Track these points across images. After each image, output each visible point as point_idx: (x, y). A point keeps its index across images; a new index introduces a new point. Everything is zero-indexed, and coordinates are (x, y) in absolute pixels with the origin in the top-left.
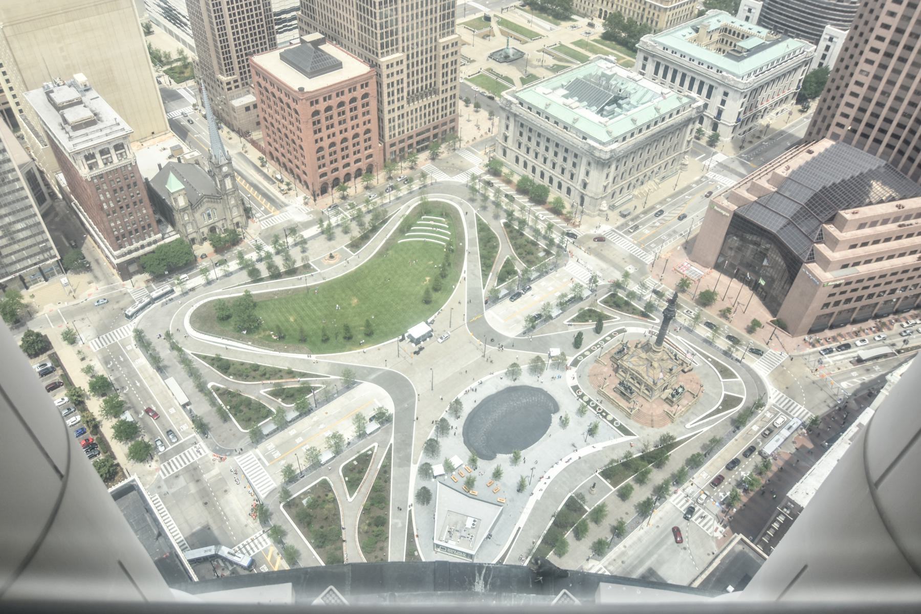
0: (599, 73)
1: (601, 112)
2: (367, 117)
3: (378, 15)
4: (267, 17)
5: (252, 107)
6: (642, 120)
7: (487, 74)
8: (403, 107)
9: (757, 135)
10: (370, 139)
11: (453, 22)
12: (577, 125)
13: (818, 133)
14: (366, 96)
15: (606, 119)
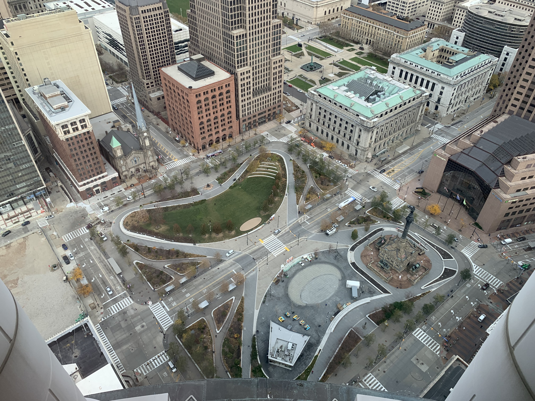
0: (366, 77)
1: (367, 100)
2: (229, 105)
3: (235, 44)
4: (170, 45)
5: (161, 98)
6: (392, 105)
8: (250, 98)
9: (463, 112)
10: (231, 117)
11: (280, 48)
12: (352, 108)
13: (500, 110)
14: (228, 92)
15: (371, 104)
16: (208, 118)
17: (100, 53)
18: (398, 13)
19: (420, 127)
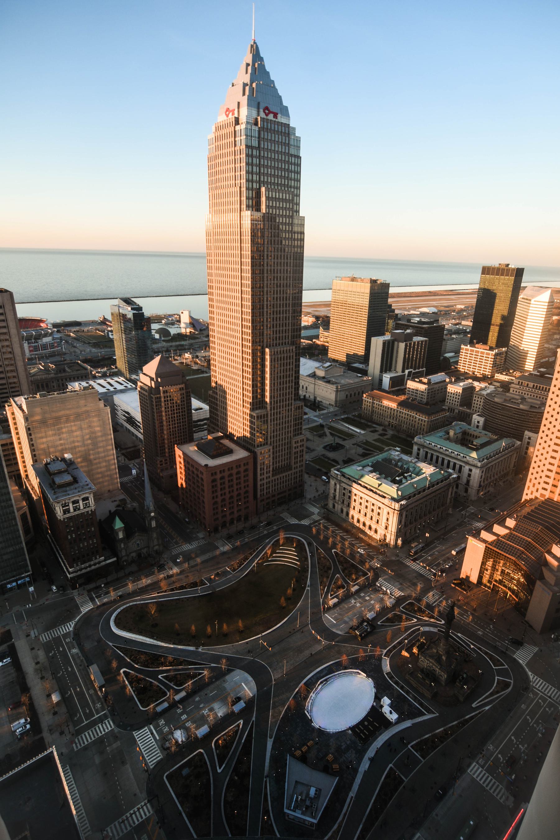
1: (394, 481)
2: (246, 484)
7: (322, 458)
8: (269, 477)
10: (248, 497)
11: (301, 428)
13: (532, 494)
14: (246, 470)
16: (223, 497)
17: (115, 430)
18: (418, 398)
19: (450, 511)
